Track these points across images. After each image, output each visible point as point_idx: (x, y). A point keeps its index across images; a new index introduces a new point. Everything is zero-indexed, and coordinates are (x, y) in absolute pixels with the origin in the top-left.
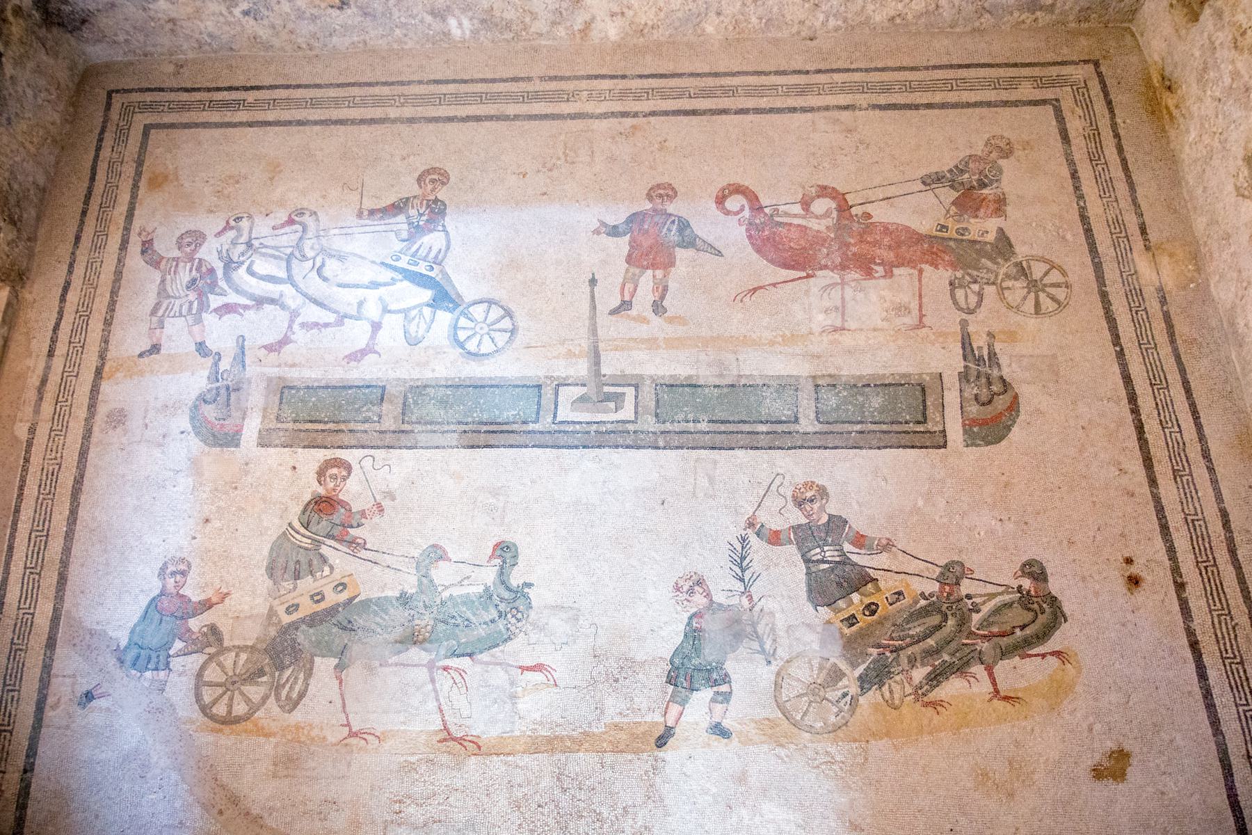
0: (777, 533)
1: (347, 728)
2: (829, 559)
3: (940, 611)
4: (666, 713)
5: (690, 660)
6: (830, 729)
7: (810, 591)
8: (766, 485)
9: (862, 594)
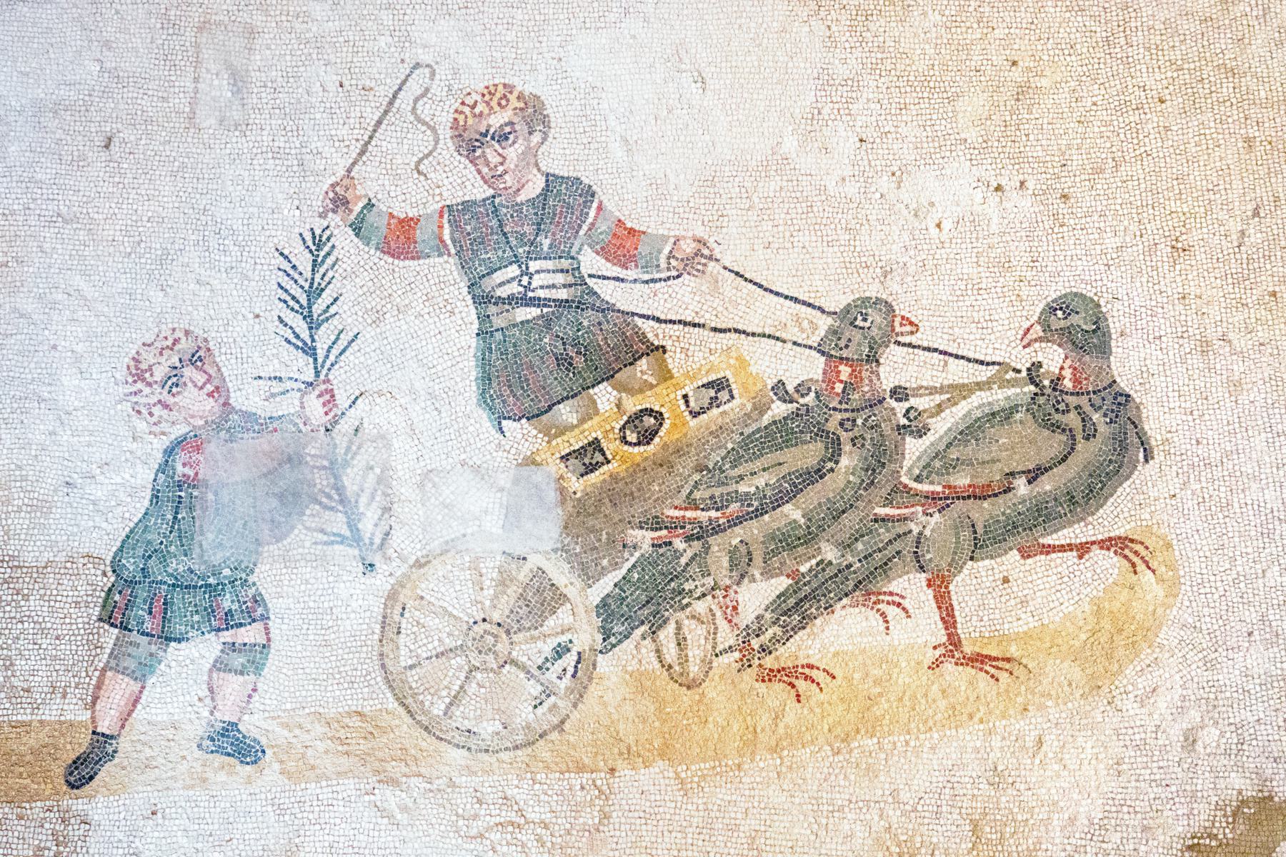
0: (407, 225)
2: (541, 294)
3: (822, 433)
4: (95, 700)
5: (164, 560)
6: (520, 738)
7: (486, 379)
8: (385, 92)
9: (621, 388)
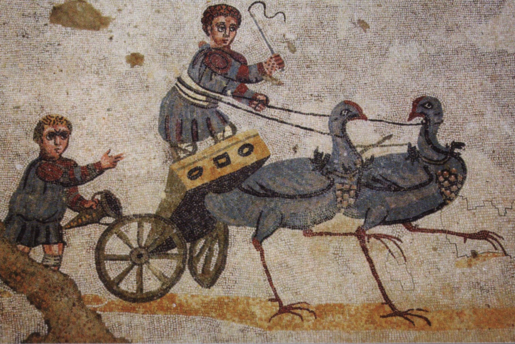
1: (277, 303)
